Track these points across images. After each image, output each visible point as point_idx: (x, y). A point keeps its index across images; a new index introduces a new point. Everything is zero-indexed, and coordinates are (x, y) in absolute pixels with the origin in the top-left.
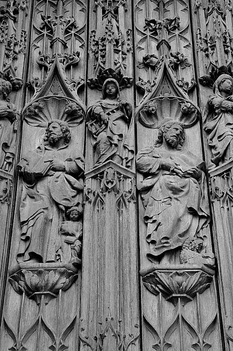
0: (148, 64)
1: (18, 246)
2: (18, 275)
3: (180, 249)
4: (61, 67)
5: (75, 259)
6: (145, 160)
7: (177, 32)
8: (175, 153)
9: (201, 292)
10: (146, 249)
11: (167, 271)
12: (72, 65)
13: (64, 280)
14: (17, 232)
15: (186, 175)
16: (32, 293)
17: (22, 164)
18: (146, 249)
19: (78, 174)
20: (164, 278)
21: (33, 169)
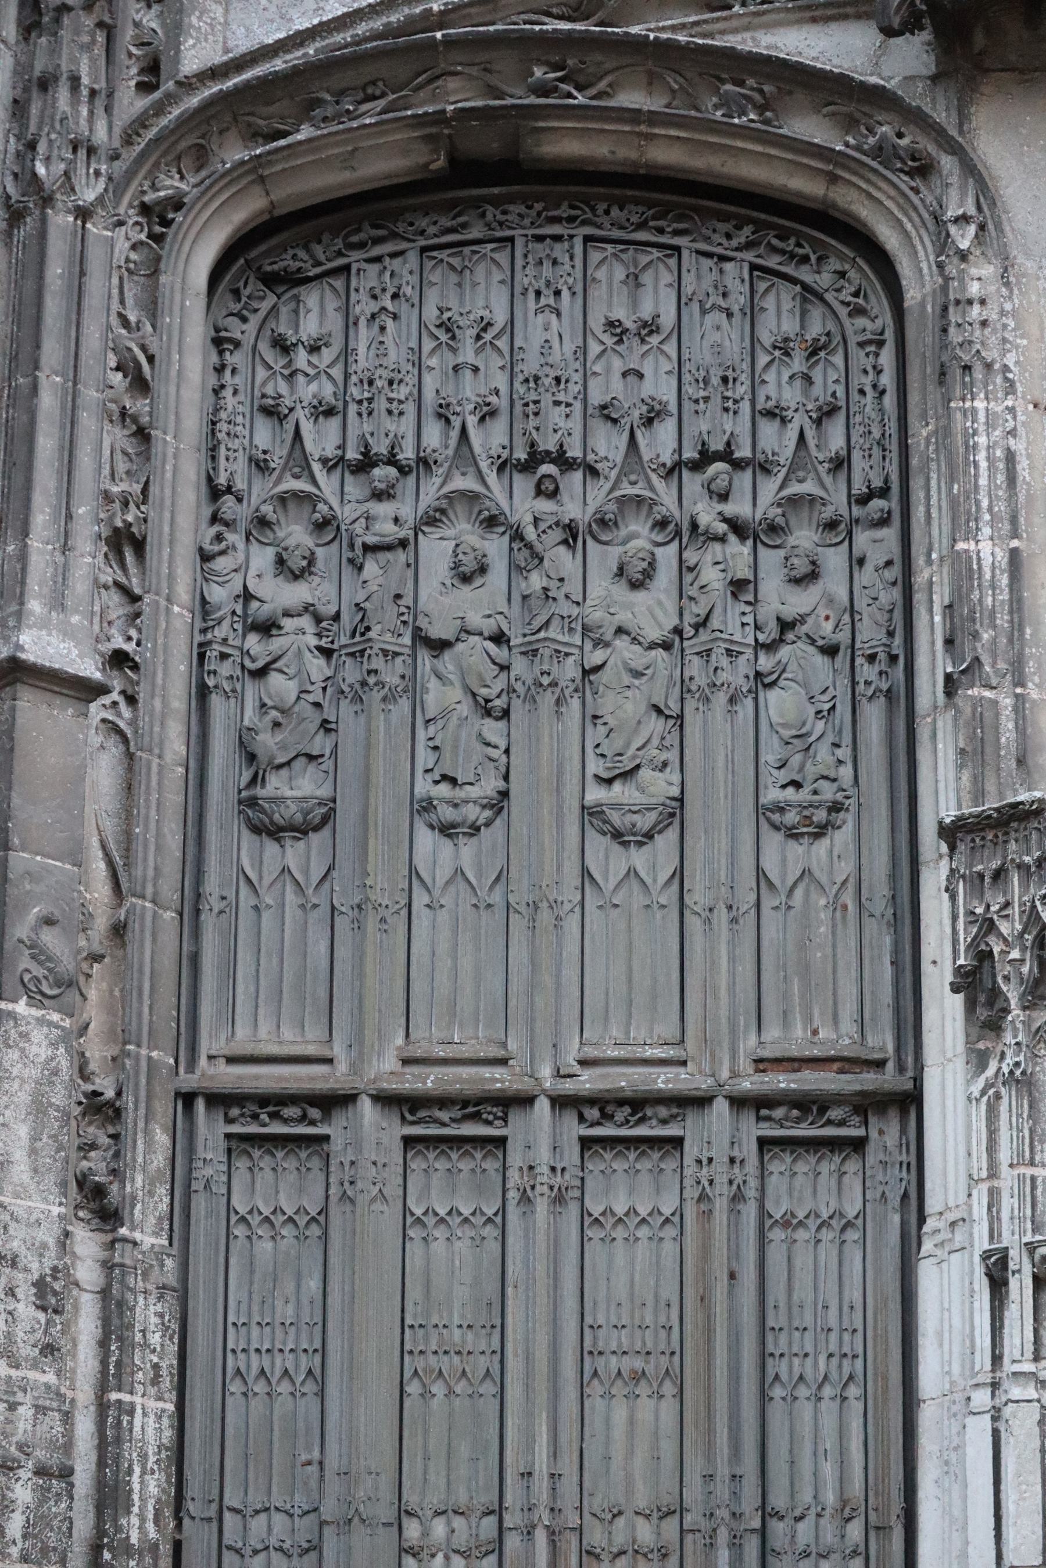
0: (607, 413)
1: (424, 757)
2: (427, 806)
3: (638, 767)
4: (472, 421)
5: (501, 784)
6: (597, 615)
7: (654, 340)
8: (640, 597)
9: (660, 832)
10: (594, 766)
11: (617, 806)
12: (487, 414)
13: (488, 813)
14: (421, 735)
15: (652, 646)
16: (447, 830)
17: (422, 622)
18: (594, 766)
19: (499, 638)
20: (615, 818)
21: (436, 632)
